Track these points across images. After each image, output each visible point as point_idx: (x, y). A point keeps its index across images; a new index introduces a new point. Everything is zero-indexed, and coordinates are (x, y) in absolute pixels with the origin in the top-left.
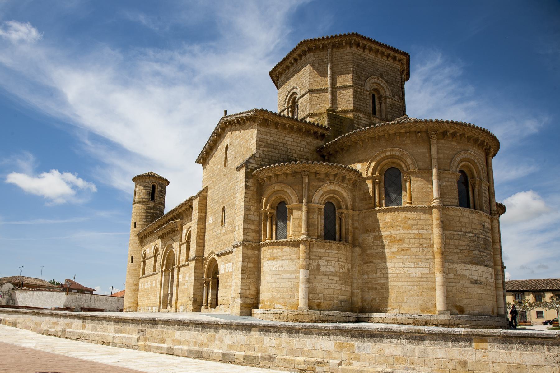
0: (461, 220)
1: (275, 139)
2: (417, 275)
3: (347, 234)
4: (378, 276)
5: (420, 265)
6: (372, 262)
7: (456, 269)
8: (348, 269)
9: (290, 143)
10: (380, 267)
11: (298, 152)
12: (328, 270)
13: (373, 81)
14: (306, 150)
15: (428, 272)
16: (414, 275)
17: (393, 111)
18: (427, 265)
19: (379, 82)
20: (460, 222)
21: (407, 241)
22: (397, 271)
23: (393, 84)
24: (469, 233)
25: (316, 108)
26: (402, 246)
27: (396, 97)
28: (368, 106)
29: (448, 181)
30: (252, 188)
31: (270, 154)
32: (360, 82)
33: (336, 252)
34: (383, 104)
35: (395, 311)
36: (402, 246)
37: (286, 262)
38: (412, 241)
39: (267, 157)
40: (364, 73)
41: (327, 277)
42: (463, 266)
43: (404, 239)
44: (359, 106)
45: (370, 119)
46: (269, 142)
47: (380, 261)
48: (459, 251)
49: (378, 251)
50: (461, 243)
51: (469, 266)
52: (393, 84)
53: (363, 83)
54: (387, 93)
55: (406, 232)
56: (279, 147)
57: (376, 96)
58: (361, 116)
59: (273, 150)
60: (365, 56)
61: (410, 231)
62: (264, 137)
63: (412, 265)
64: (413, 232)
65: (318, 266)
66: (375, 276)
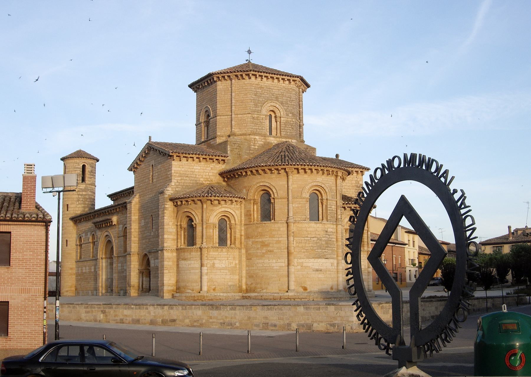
0: (308, 229)
1: (186, 169)
2: (277, 268)
3: (235, 239)
4: (255, 268)
5: (279, 261)
6: (251, 259)
7: (302, 263)
8: (236, 264)
9: (198, 170)
10: (256, 262)
11: (204, 176)
12: (220, 266)
13: (269, 105)
14: (210, 174)
15: (284, 265)
16: (275, 268)
17: (286, 128)
18: (283, 261)
19: (274, 104)
20: (307, 231)
21: (271, 245)
22: (265, 265)
23: (287, 104)
24: (313, 238)
25: (222, 131)
26: (269, 249)
27: (290, 115)
28: (263, 128)
29: (300, 204)
30: (170, 209)
31: (183, 181)
32: (257, 109)
33: (226, 253)
34: (278, 123)
35: (264, 291)
36: (269, 249)
37: (193, 262)
38: (274, 245)
39: (181, 184)
40: (261, 100)
41: (219, 271)
42: (307, 260)
43: (270, 243)
44: (255, 130)
45: (265, 139)
46: (182, 172)
47: (255, 258)
48: (305, 251)
49: (254, 251)
50: (307, 245)
51: (312, 260)
52: (287, 104)
53: (260, 109)
54: (282, 113)
55: (271, 239)
56: (189, 175)
57: (273, 115)
58: (257, 137)
59: (184, 178)
60: (263, 84)
61: (274, 239)
62: (178, 169)
63: (274, 261)
64: (275, 239)
65: (214, 264)
66: (252, 268)
